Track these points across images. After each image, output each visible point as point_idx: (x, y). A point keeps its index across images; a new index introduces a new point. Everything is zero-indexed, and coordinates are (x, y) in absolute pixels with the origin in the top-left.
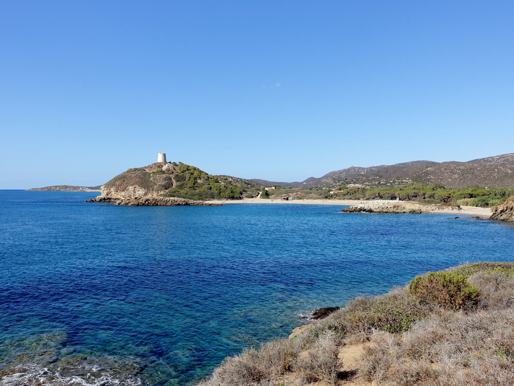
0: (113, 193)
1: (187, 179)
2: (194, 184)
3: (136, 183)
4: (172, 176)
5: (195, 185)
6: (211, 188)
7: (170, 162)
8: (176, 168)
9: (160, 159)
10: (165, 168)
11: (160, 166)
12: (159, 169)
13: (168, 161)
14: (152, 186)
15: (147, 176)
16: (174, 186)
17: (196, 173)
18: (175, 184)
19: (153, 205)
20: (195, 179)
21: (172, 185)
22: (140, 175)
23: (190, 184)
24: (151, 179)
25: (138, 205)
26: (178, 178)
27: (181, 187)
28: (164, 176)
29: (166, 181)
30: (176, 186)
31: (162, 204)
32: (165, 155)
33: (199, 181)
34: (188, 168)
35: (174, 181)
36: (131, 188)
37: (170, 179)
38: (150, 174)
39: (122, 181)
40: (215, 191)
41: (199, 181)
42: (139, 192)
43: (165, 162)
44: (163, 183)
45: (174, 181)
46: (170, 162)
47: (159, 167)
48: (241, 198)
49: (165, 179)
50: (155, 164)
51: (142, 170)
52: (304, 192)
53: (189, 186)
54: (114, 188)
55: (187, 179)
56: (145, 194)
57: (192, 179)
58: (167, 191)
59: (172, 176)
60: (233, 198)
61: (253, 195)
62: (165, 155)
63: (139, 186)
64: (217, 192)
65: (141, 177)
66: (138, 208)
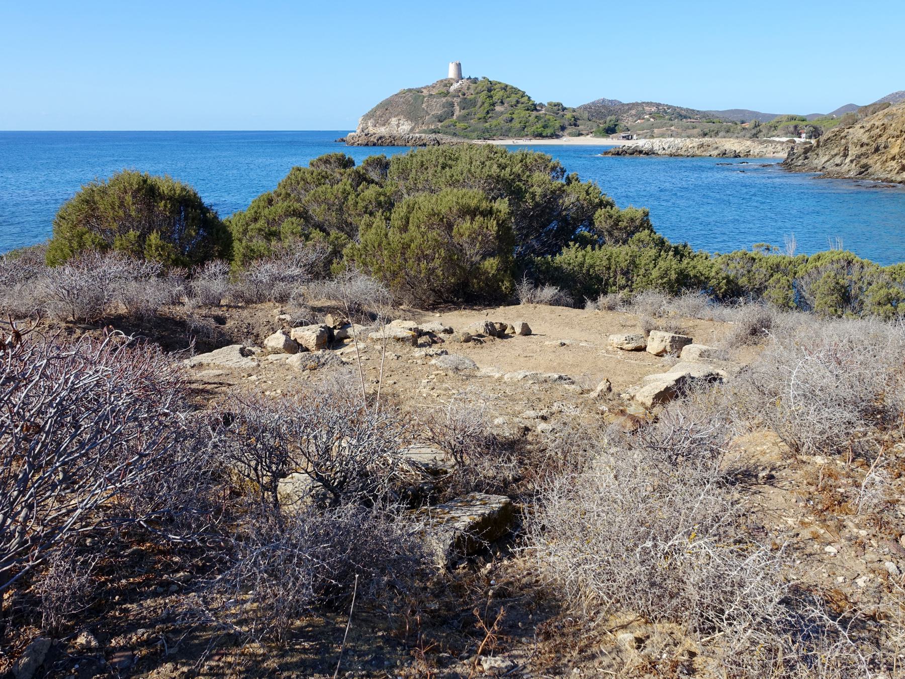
0: (371, 128)
2: (488, 113)
3: (402, 113)
5: (490, 115)
6: (511, 120)
7: (470, 78)
8: (473, 86)
9: (452, 73)
10: (456, 86)
11: (448, 83)
12: (444, 90)
13: (465, 75)
14: (421, 118)
16: (455, 117)
17: (498, 95)
18: (457, 113)
19: (374, 145)
20: (493, 104)
23: (481, 113)
25: (367, 145)
26: (467, 104)
27: (464, 118)
28: (444, 100)
30: (458, 118)
31: (400, 143)
32: (459, 66)
33: (498, 108)
34: (491, 87)
35: (457, 108)
36: (394, 121)
37: (452, 105)
38: (424, 97)
40: (516, 124)
41: (498, 108)
42: (404, 127)
45: (457, 108)
46: (470, 78)
47: (445, 85)
48: (558, 137)
50: (442, 81)
51: (419, 91)
52: (682, 126)
53: (478, 116)
54: (372, 120)
55: (479, 104)
56: (412, 130)
57: (486, 105)
58: (440, 124)
60: (540, 136)
62: (459, 66)
64: (519, 125)
65: (410, 103)
66: (366, 148)
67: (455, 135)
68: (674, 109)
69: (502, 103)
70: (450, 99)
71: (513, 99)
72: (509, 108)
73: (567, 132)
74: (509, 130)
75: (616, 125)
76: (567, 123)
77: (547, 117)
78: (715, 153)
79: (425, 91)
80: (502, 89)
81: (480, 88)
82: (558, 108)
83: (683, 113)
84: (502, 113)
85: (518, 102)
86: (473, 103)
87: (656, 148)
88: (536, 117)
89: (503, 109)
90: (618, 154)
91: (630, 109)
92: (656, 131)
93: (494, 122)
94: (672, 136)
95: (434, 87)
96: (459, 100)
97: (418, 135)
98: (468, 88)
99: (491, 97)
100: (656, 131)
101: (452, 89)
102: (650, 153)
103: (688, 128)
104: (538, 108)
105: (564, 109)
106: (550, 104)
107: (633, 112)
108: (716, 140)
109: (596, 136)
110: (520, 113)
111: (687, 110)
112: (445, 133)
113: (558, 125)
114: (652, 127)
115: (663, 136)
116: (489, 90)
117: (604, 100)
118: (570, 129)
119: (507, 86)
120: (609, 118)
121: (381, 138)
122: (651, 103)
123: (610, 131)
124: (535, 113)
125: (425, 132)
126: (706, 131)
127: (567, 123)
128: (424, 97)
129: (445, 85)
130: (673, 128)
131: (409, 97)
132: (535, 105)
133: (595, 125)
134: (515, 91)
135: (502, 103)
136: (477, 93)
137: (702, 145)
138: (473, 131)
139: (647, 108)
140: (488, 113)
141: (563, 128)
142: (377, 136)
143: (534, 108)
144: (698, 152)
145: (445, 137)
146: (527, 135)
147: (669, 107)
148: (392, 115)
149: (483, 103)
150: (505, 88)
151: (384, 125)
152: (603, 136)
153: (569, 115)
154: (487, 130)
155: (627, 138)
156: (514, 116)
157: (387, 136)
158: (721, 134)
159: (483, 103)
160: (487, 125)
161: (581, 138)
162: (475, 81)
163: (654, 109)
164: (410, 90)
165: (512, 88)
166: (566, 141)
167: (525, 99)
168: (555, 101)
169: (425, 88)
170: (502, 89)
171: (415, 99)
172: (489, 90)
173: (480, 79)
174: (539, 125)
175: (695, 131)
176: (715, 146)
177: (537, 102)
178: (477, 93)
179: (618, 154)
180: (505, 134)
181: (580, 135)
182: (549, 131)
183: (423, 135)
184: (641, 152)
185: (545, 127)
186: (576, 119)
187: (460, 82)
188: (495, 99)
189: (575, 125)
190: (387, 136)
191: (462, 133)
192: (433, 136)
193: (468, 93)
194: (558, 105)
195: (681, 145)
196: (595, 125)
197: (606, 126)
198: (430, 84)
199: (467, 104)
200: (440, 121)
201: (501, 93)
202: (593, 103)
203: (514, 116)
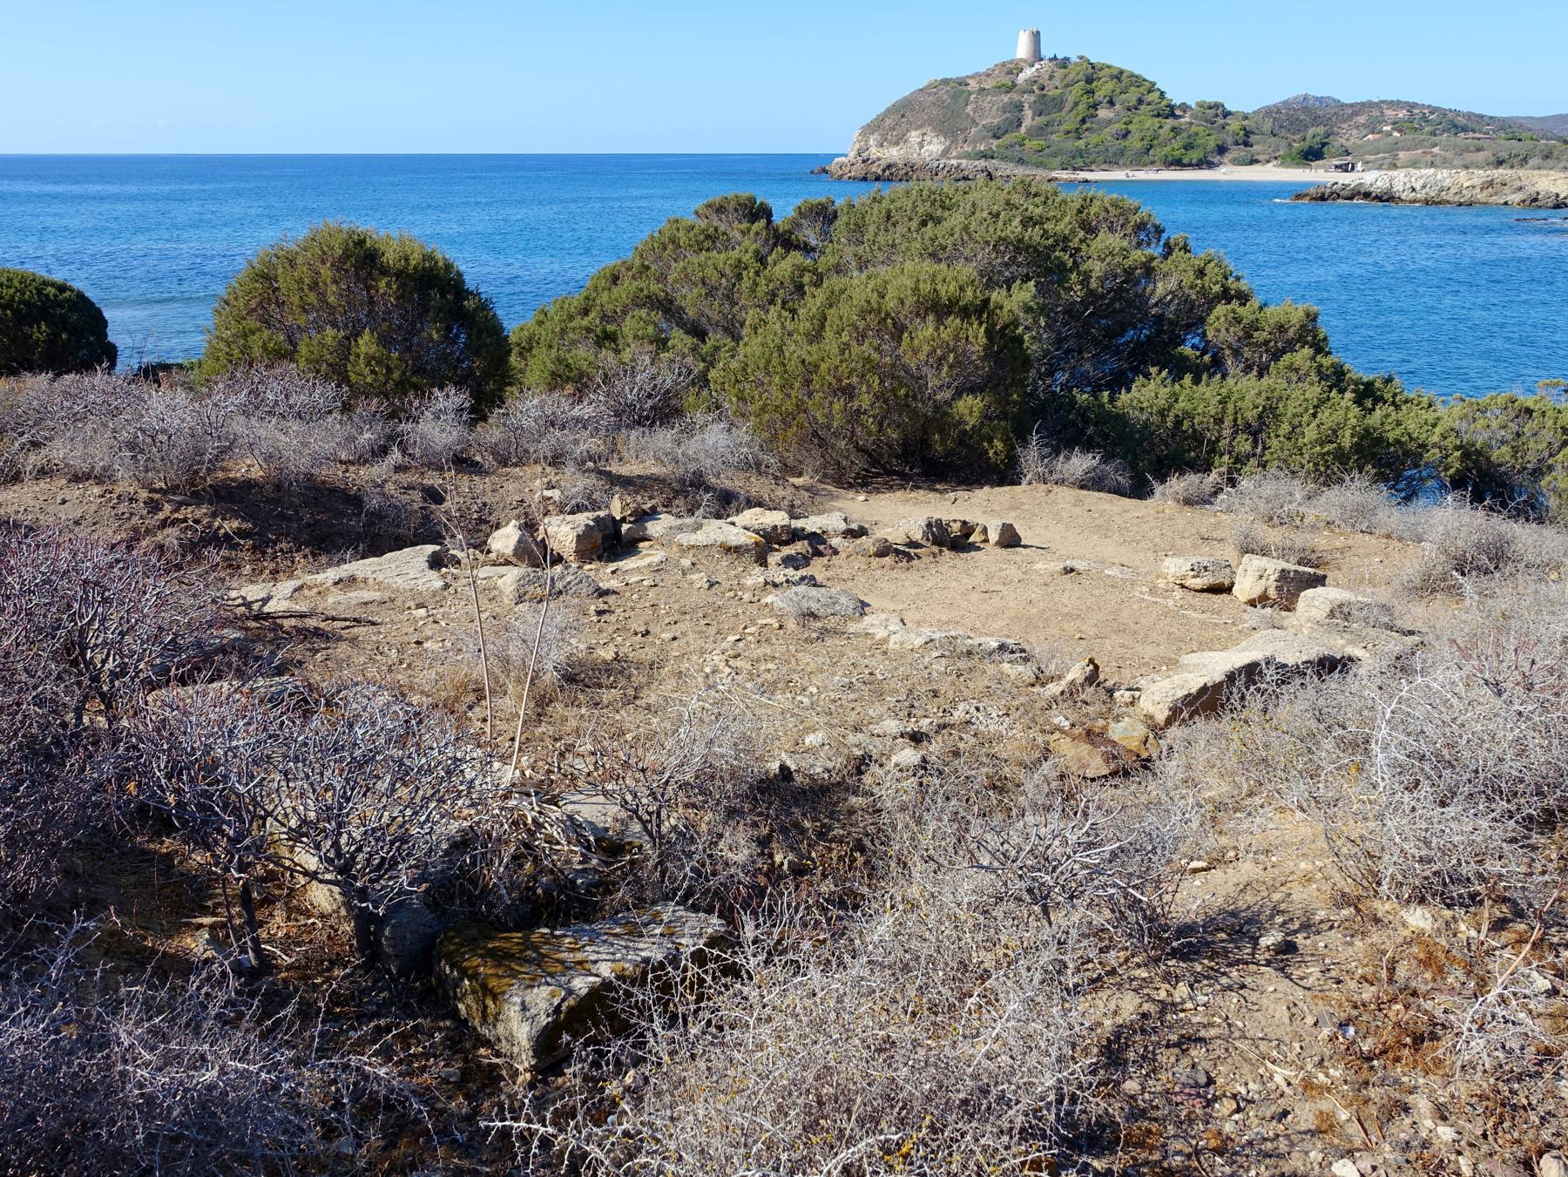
0: (873, 150)
2: (1083, 121)
3: (929, 122)
5: (1087, 125)
7: (1055, 58)
8: (1060, 72)
9: (1022, 50)
10: (1029, 73)
11: (1014, 68)
12: (1007, 80)
13: (1047, 52)
15: (961, 101)
16: (1023, 130)
17: (1104, 89)
18: (1029, 120)
19: (877, 179)
20: (1095, 106)
23: (1071, 122)
24: (969, 109)
25: (865, 179)
26: (1047, 105)
27: (1040, 131)
30: (1028, 130)
32: (1036, 36)
33: (1103, 113)
34: (1092, 74)
35: (1028, 113)
36: (914, 136)
37: (1019, 107)
38: (970, 93)
39: (898, 118)
40: (1135, 143)
43: (1037, 56)
45: (1028, 113)
46: (1055, 58)
47: (1010, 72)
48: (1211, 165)
50: (1004, 65)
51: (962, 82)
52: (1455, 145)
53: (1065, 127)
54: (876, 135)
56: (945, 153)
57: (1081, 107)
58: (995, 142)
60: (1178, 163)
61: (1260, 158)
62: (1036, 36)
64: (1139, 145)
65: (944, 105)
66: (863, 184)
67: (1021, 161)
68: (1443, 113)
69: (1111, 103)
70: (1015, 96)
71: (1132, 96)
72: (1123, 113)
73: (1228, 156)
74: (1122, 153)
75: (1324, 144)
76: (1229, 140)
77: (1194, 129)
78: (1516, 198)
79: (973, 83)
80: (1113, 77)
81: (1072, 75)
82: (1216, 113)
83: (1461, 121)
84: (1110, 122)
85: (1140, 101)
86: (1058, 104)
87: (1398, 187)
88: (1173, 129)
89: (1111, 115)
90: (1322, 198)
91: (1356, 114)
92: (1402, 155)
93: (1093, 139)
94: (1432, 165)
95: (988, 75)
96: (1032, 98)
97: (954, 162)
98: (1051, 77)
99: (1092, 92)
100: (1402, 155)
101: (1022, 77)
102: (1387, 198)
103: (1467, 150)
104: (1178, 112)
105: (1227, 114)
106: (1200, 105)
107: (1362, 119)
108: (1521, 172)
109: (1283, 165)
110: (1145, 122)
111: (1469, 115)
112: (1004, 158)
113: (1212, 143)
114: (1394, 148)
115: (1414, 164)
116: (1089, 80)
117: (1305, 98)
118: (1235, 152)
119: (1122, 72)
120: (1311, 131)
121: (889, 167)
122: (1399, 102)
123: (1312, 155)
124: (1170, 122)
125: (967, 156)
126: (1503, 155)
127: (1229, 140)
128: (970, 93)
129: (1010, 72)
130: (1436, 150)
131: (944, 93)
132: (1172, 107)
133: (1284, 143)
134: (1137, 81)
135: (1111, 103)
136: (1067, 86)
137: (1491, 184)
138: (1054, 155)
139: (1389, 113)
140: (1083, 121)
141: (1222, 150)
142: (884, 163)
143: (1171, 112)
144: (1482, 197)
145: (1003, 165)
146: (1153, 163)
147: (1433, 110)
148: (911, 126)
149: (1076, 104)
150: (1119, 75)
151: (897, 144)
152: (1298, 165)
153: (1234, 125)
154: (1080, 153)
155: (1344, 168)
156: (1130, 127)
157: (900, 163)
158: (1531, 162)
159: (1076, 104)
160: (1081, 143)
161: (1256, 167)
162: (1064, 63)
163: (1402, 114)
164: (946, 82)
165: (1132, 75)
166: (1227, 173)
167: (1154, 96)
168: (1211, 98)
169: (972, 77)
170: (1113, 77)
171: (954, 97)
172: (1089, 80)
173: (1074, 59)
174: (1177, 144)
175: (1481, 156)
176: (1517, 184)
177: (1177, 101)
178: (1067, 86)
179: (1322, 198)
180: (1112, 162)
181: (1253, 162)
182: (1194, 155)
183: (964, 162)
184: (1367, 195)
185: (1188, 147)
186: (1248, 133)
187: (1037, 66)
188: (1099, 96)
189: (1246, 144)
190: (900, 163)
191: (1034, 158)
192: (982, 163)
193: (1049, 85)
194: (1217, 106)
195: (1447, 183)
196: (1284, 143)
197: (1306, 145)
198: (982, 70)
199: (1047, 105)
200: (996, 137)
201: (1111, 85)
202: (1285, 103)
203: (1130, 127)
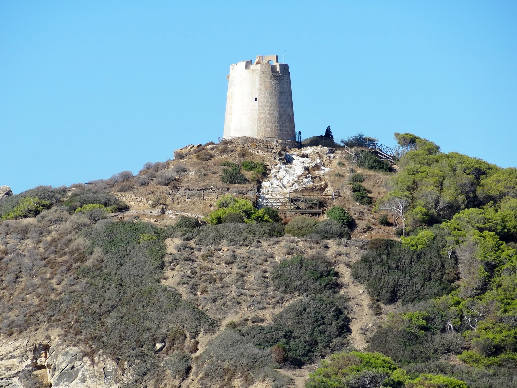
1: (469, 278)
3: (51, 311)
4: (344, 255)
7: (326, 139)
9: (244, 116)
10: (282, 184)
11: (242, 167)
13: (307, 127)
14: (173, 339)
15: (140, 254)
16: (357, 340)
21: (344, 329)
22: (80, 241)
24: (172, 278)
26: (395, 272)
28: (279, 250)
29: (296, 299)
30: (378, 340)
32: (281, 78)
35: (357, 295)
37: (327, 277)
38: (161, 235)
44: (268, 315)
45: (357, 295)
46: (326, 139)
47: (234, 177)
49: (284, 281)
50: (202, 153)
53: (481, 334)
59: (344, 255)
62: (281, 78)
63: (73, 334)
96: (355, 255)
149: (492, 268)
159: (492, 268)
162: (367, 153)
